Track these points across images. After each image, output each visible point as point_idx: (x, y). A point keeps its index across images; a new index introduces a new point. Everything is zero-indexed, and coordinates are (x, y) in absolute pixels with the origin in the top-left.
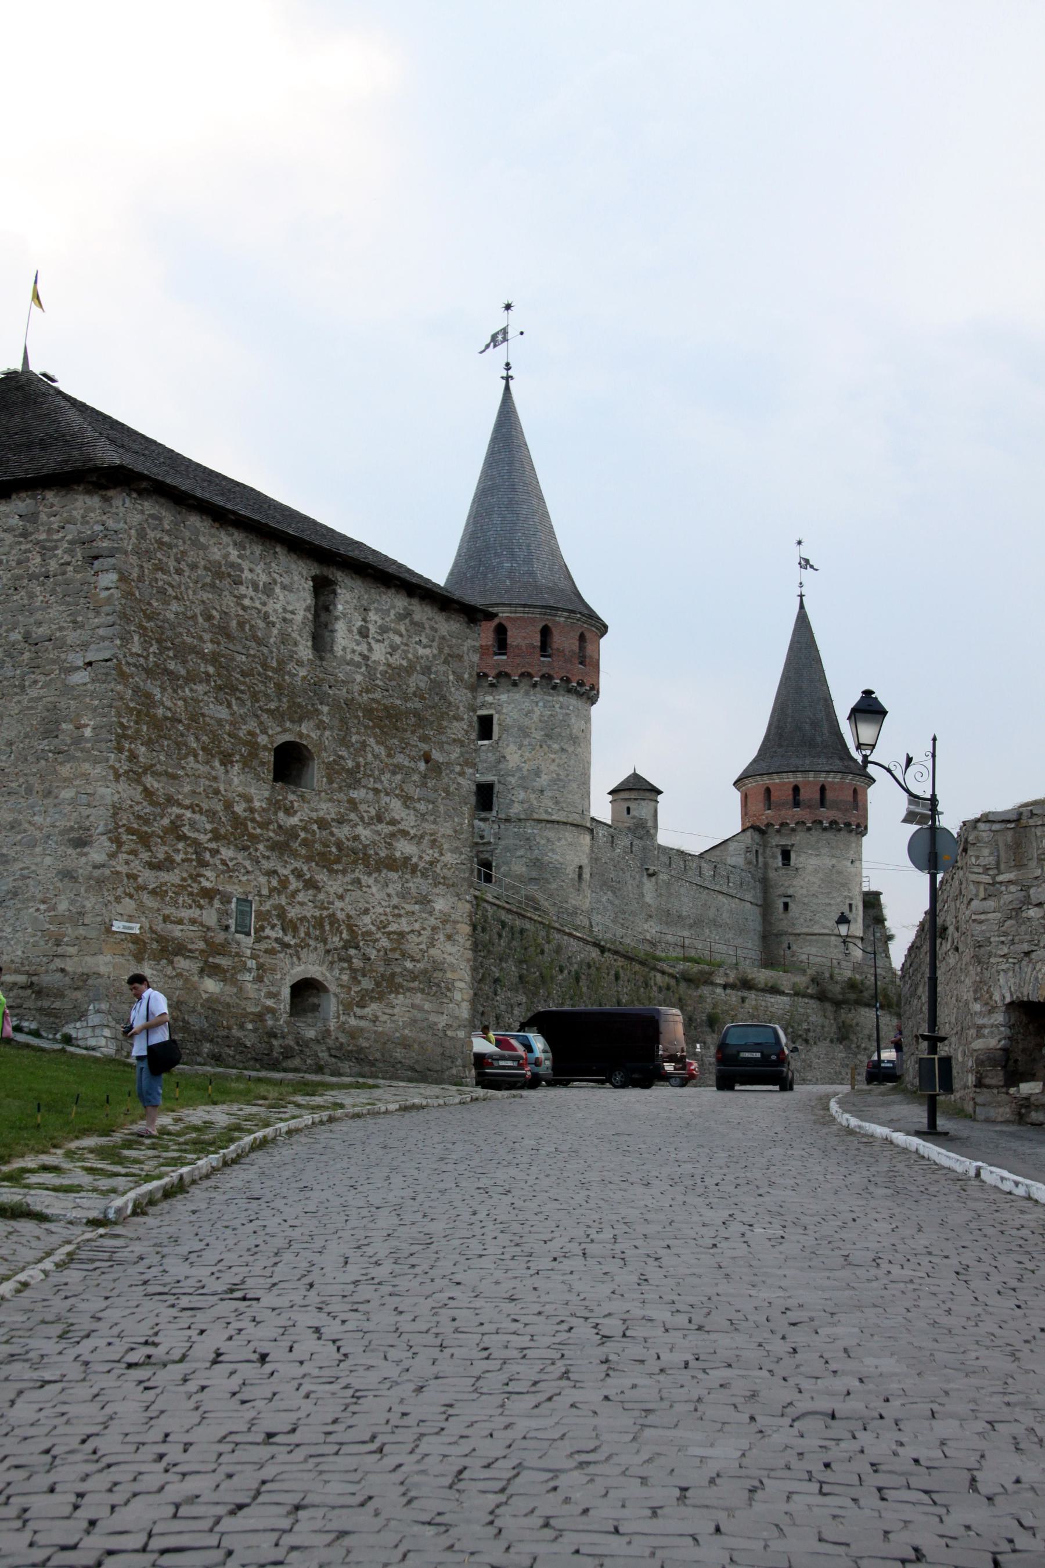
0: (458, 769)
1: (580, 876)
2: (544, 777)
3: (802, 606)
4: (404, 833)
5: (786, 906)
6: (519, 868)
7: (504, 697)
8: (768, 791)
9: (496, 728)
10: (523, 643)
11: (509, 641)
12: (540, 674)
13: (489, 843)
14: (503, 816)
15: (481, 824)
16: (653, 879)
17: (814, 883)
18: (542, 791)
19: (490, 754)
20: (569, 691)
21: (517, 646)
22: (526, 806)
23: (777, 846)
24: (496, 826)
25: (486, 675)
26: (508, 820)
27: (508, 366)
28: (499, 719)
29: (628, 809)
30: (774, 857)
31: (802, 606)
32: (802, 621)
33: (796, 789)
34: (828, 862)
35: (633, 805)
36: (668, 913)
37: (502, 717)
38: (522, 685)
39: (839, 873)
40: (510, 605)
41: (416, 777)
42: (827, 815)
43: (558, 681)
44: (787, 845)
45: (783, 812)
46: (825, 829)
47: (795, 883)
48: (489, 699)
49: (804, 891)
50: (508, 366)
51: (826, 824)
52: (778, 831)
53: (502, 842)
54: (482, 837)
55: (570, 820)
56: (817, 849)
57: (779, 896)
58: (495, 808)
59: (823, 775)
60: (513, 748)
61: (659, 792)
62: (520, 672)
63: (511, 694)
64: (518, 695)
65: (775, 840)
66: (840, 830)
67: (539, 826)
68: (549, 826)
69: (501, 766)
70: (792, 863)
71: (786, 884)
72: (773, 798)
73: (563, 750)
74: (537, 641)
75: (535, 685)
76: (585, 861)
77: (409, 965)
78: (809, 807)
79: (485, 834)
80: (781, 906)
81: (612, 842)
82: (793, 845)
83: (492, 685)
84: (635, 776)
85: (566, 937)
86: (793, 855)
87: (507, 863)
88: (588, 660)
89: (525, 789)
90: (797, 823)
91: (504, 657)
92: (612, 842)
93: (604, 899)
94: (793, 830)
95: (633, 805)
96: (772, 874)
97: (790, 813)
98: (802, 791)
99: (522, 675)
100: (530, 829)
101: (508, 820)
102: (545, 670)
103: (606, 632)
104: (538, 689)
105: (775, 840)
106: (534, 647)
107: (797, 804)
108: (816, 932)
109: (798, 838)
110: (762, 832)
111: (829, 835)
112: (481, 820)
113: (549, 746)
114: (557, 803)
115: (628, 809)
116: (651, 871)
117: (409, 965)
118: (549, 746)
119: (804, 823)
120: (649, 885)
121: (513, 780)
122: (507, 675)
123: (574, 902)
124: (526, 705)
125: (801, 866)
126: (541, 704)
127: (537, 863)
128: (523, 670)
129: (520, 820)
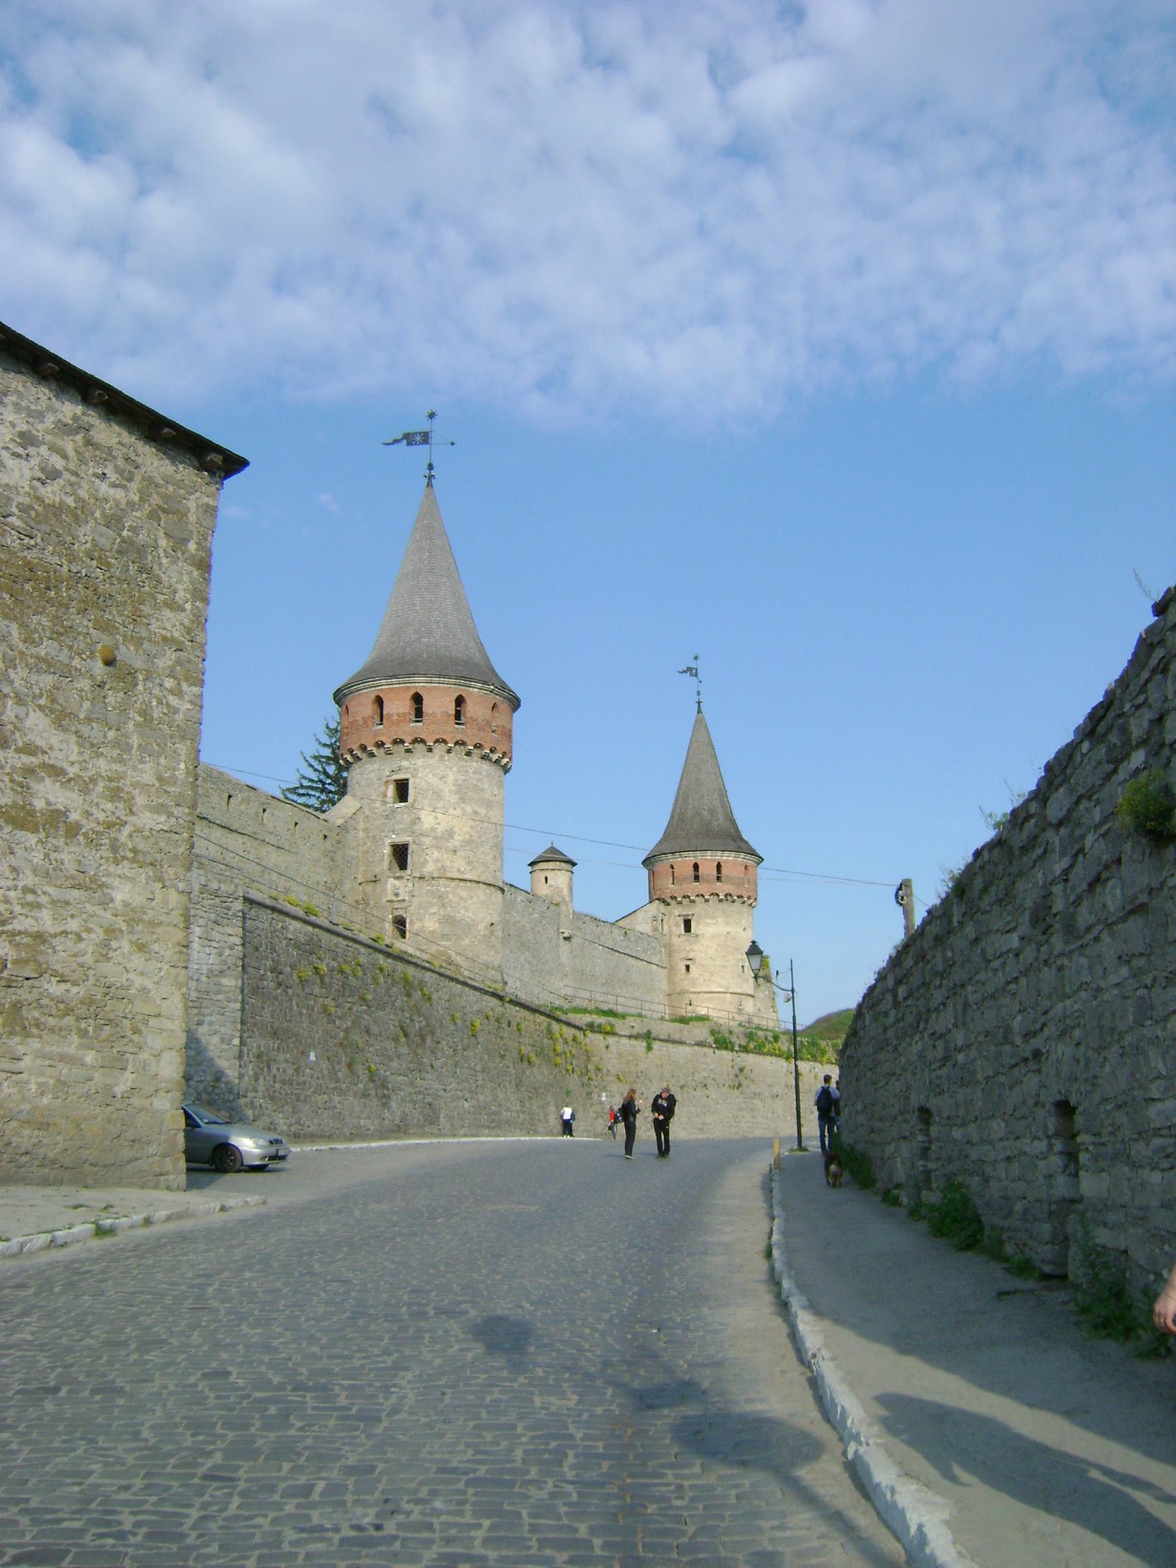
0: (169, 683)
2: (457, 837)
4: (56, 772)
5: (688, 967)
6: (431, 924)
7: (420, 762)
13: (404, 900)
14: (418, 875)
15: (397, 882)
19: (405, 816)
20: (485, 757)
22: (439, 865)
25: (402, 742)
26: (422, 878)
27: (431, 467)
34: (724, 929)
35: (549, 875)
36: (582, 972)
37: (418, 781)
39: (734, 939)
40: (425, 675)
41: (85, 684)
42: (722, 888)
45: (684, 886)
47: (695, 947)
48: (405, 763)
49: (703, 955)
50: (431, 467)
51: (722, 897)
53: (416, 901)
54: (397, 895)
55: (482, 880)
56: (714, 918)
59: (719, 853)
63: (426, 760)
64: (433, 759)
66: (734, 901)
67: (453, 884)
68: (461, 884)
69: (416, 827)
71: (688, 948)
73: (476, 812)
74: (451, 709)
75: (449, 751)
77: (55, 989)
78: (707, 881)
79: (400, 891)
83: (408, 751)
84: (553, 850)
85: (459, 986)
87: (420, 920)
89: (439, 848)
95: (549, 875)
99: (437, 741)
100: (442, 886)
101: (422, 878)
102: (459, 737)
103: (519, 706)
104: (453, 754)
106: (449, 715)
109: (697, 910)
111: (725, 906)
113: (463, 809)
114: (469, 863)
117: (55, 989)
118: (463, 809)
120: (565, 947)
121: (427, 841)
122: (423, 741)
126: (455, 769)
127: (449, 920)
129: (433, 878)
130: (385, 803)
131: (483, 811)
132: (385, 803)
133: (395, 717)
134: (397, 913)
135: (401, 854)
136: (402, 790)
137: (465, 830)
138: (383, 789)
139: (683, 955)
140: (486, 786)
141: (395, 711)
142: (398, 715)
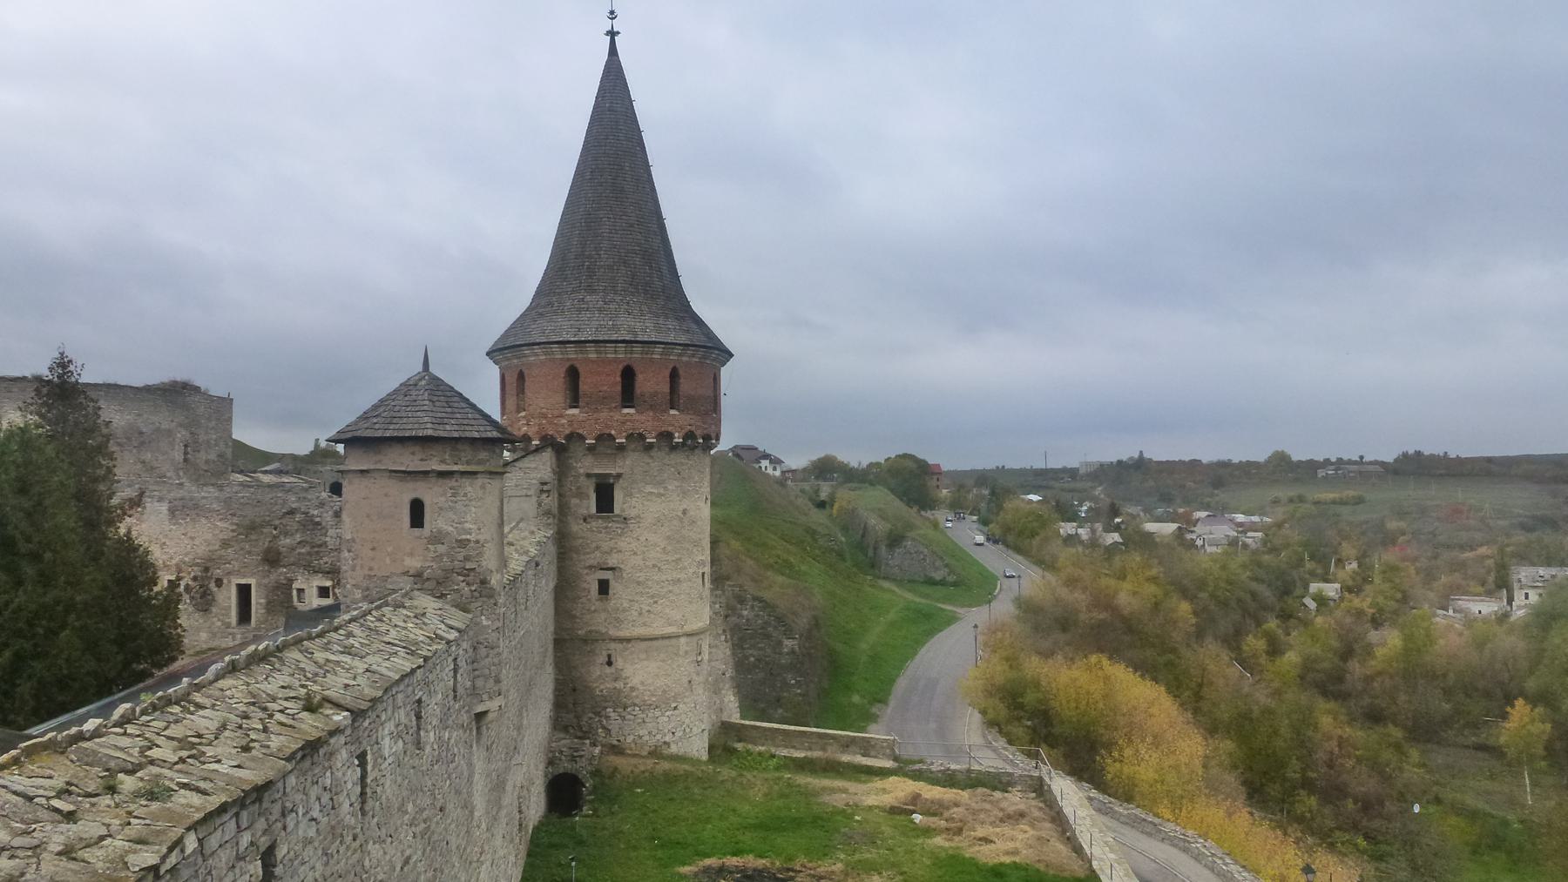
3: (613, 51)
5: (604, 587)
8: (573, 374)
17: (656, 545)
23: (589, 476)
29: (417, 513)
30: (585, 496)
31: (613, 51)
32: (614, 80)
33: (628, 375)
35: (432, 496)
42: (678, 421)
44: (609, 475)
45: (604, 415)
46: (674, 448)
47: (622, 544)
49: (638, 560)
52: (591, 449)
57: (590, 567)
65: (585, 465)
66: (693, 448)
70: (617, 511)
71: (605, 546)
72: (583, 387)
78: (652, 407)
80: (595, 587)
82: (619, 476)
86: (618, 496)
90: (629, 437)
94: (621, 448)
95: (432, 496)
96: (576, 527)
97: (617, 417)
98: (640, 378)
105: (585, 465)
107: (628, 396)
108: (658, 632)
109: (627, 464)
110: (560, 450)
111: (678, 458)
115: (417, 513)
119: (642, 437)
125: (633, 513)
139: (594, 558)
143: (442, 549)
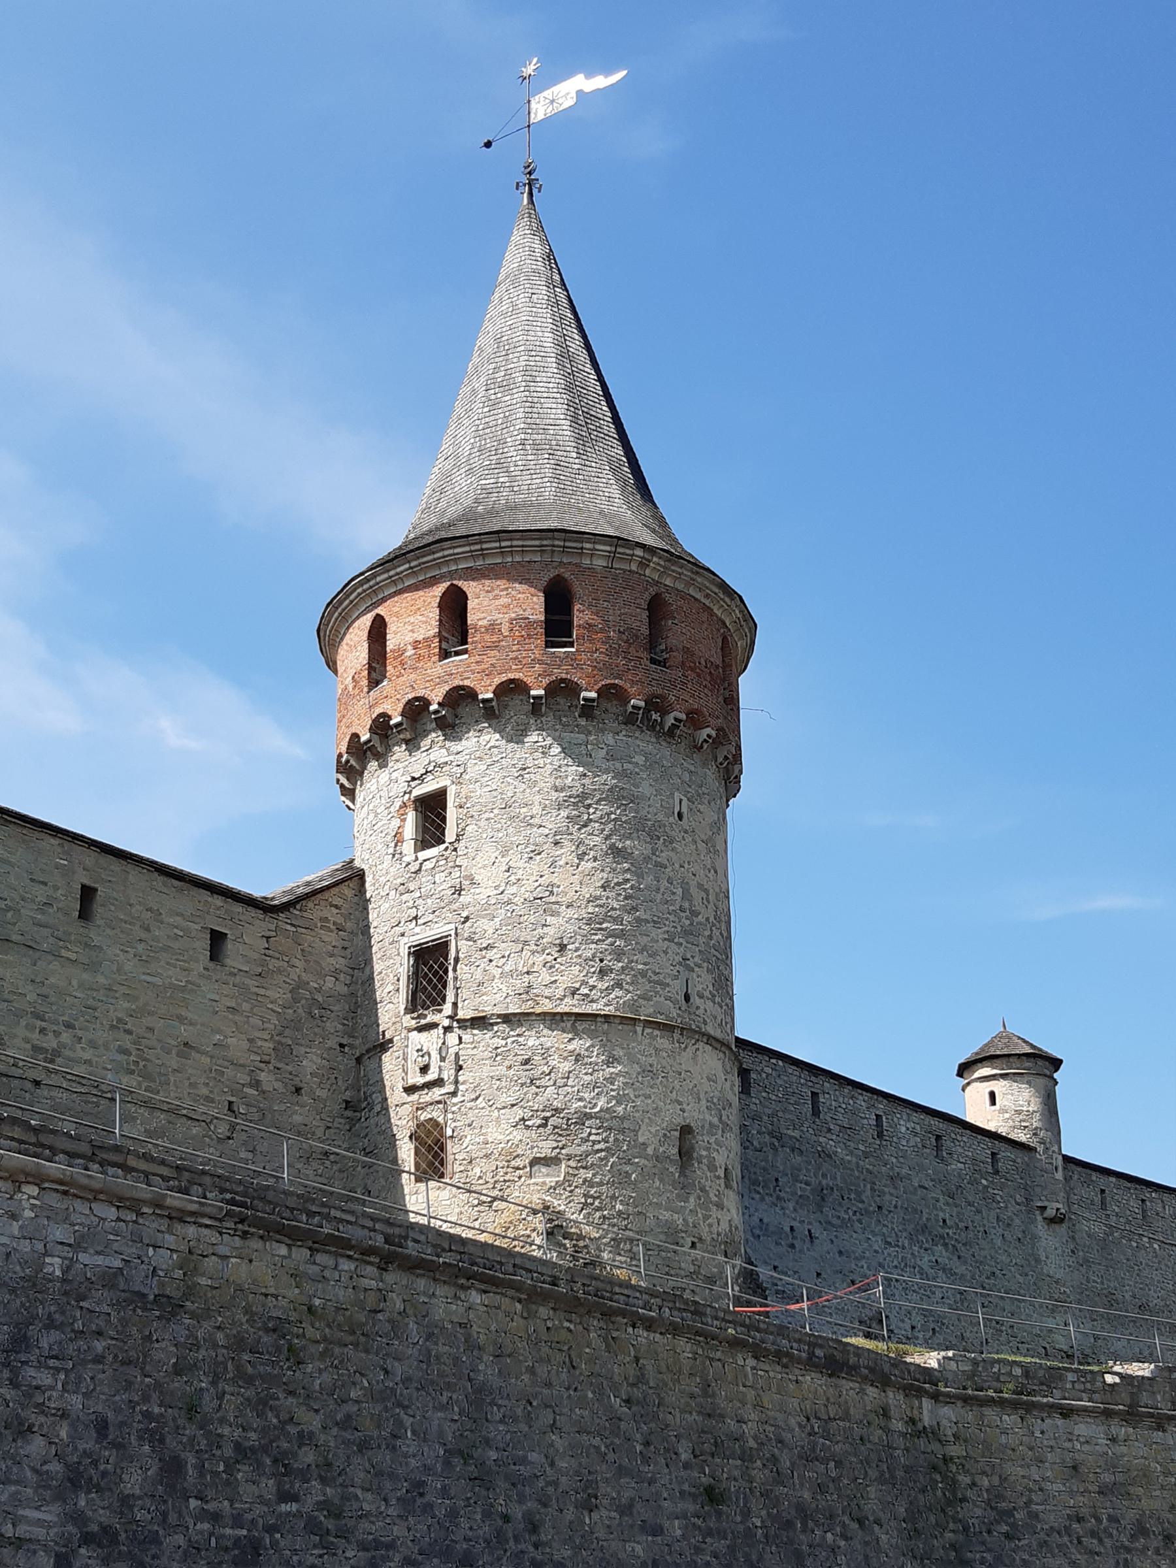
1: (685, 1154)
9: (451, 814)
10: (503, 619)
11: (471, 619)
12: (546, 681)
16: (1062, 1229)
18: (562, 948)
19: (439, 878)
20: (630, 720)
21: (492, 628)
24: (452, 1039)
28: (458, 795)
29: (992, 1096)
38: (507, 714)
43: (593, 695)
58: (450, 998)
60: (489, 852)
61: (1056, 1063)
62: (497, 681)
76: (696, 1114)
81: (938, 1148)
88: (677, 657)
91: (466, 656)
92: (938, 1148)
93: (925, 1261)
95: (999, 1086)
102: (560, 673)
106: (530, 624)
112: (421, 1029)
115: (992, 1096)
116: (1051, 1213)
120: (1049, 1241)
121: (486, 927)
123: (665, 1215)
124: (519, 754)
128: (504, 677)
130: (397, 855)
131: (636, 846)
132: (397, 855)
133: (410, 652)
134: (424, 1116)
135: (431, 966)
136: (431, 811)
137: (586, 892)
138: (396, 823)
140: (646, 789)
141: (410, 638)
142: (416, 644)
143: (1007, 1116)
